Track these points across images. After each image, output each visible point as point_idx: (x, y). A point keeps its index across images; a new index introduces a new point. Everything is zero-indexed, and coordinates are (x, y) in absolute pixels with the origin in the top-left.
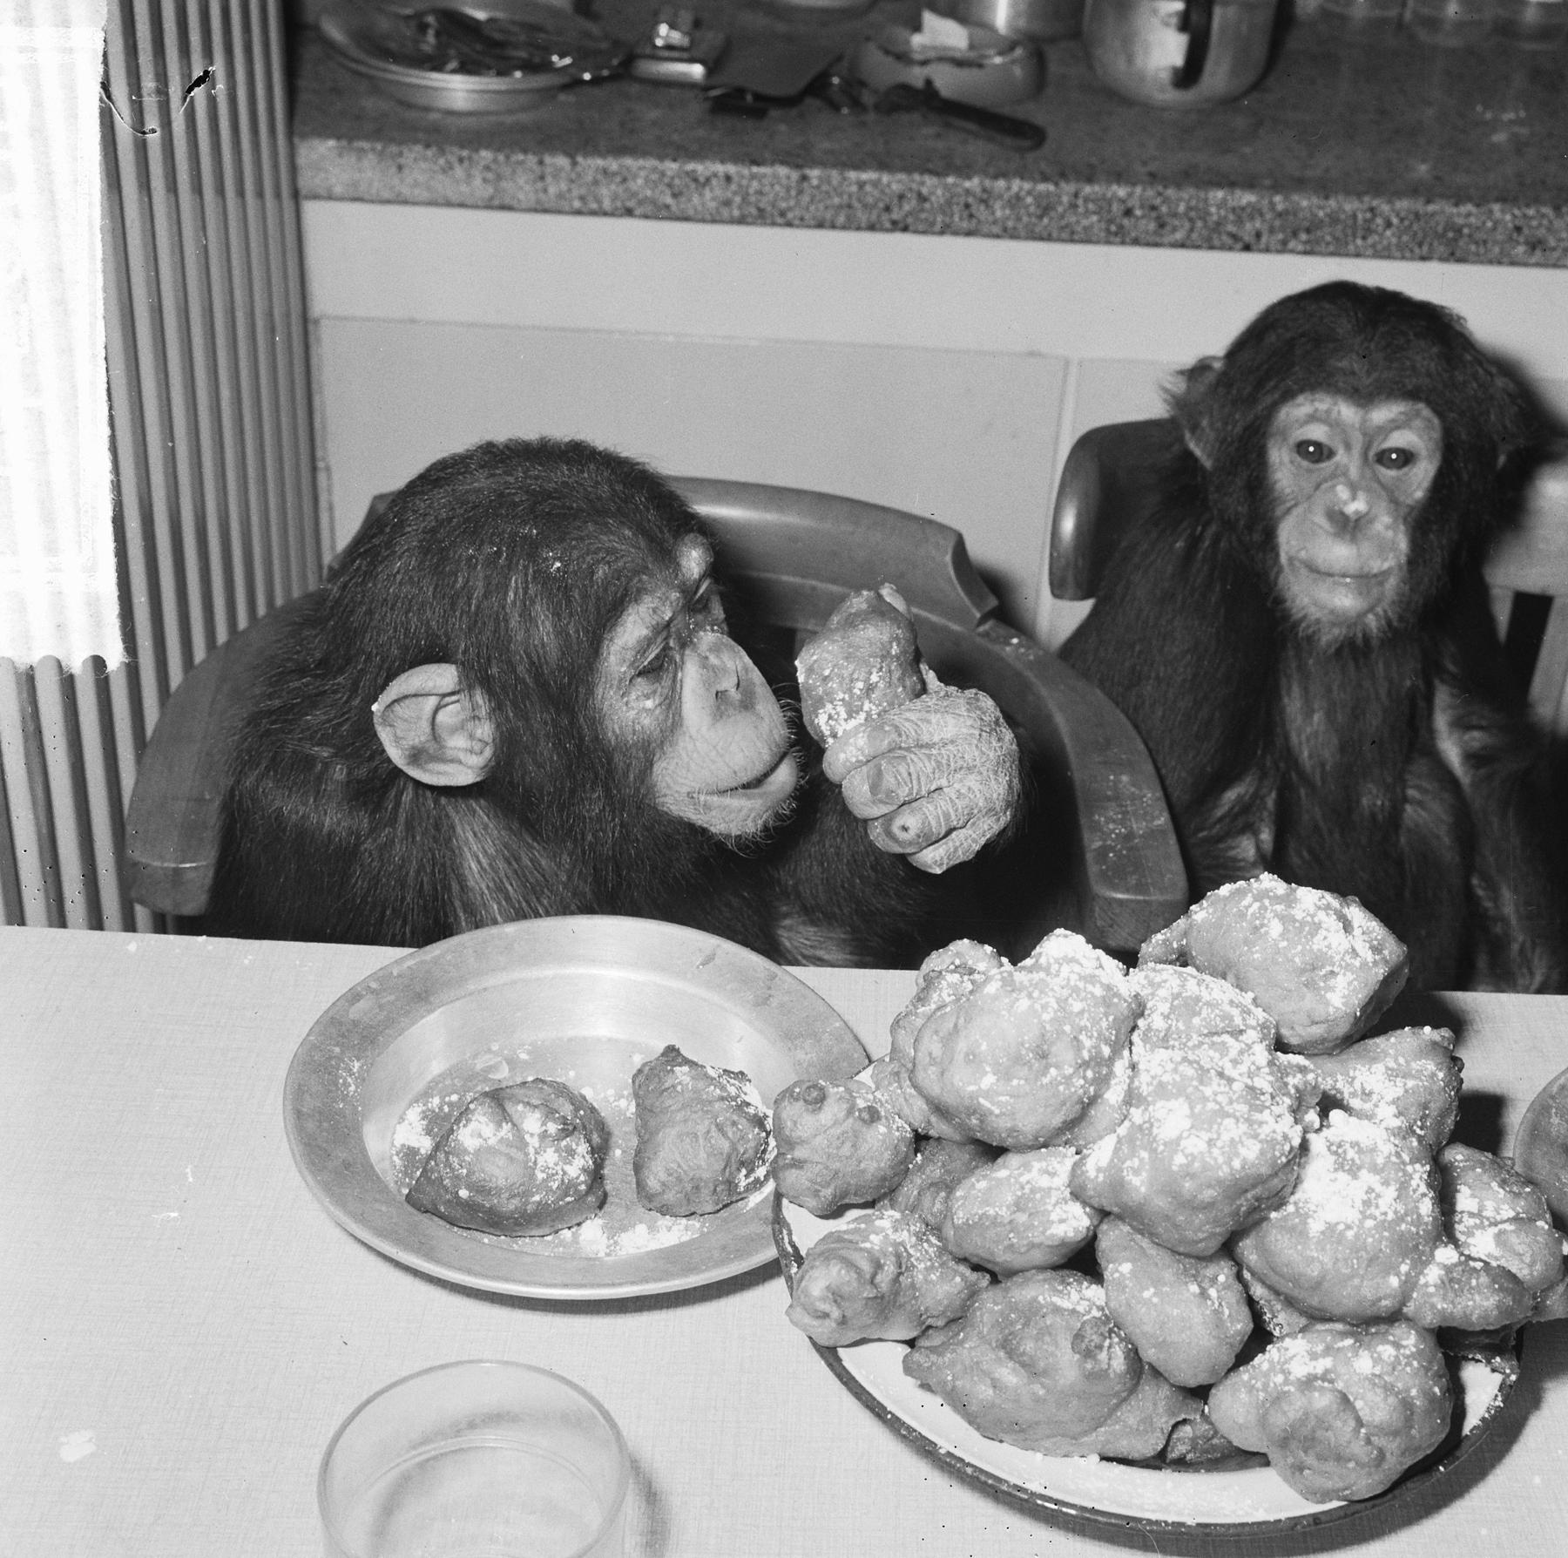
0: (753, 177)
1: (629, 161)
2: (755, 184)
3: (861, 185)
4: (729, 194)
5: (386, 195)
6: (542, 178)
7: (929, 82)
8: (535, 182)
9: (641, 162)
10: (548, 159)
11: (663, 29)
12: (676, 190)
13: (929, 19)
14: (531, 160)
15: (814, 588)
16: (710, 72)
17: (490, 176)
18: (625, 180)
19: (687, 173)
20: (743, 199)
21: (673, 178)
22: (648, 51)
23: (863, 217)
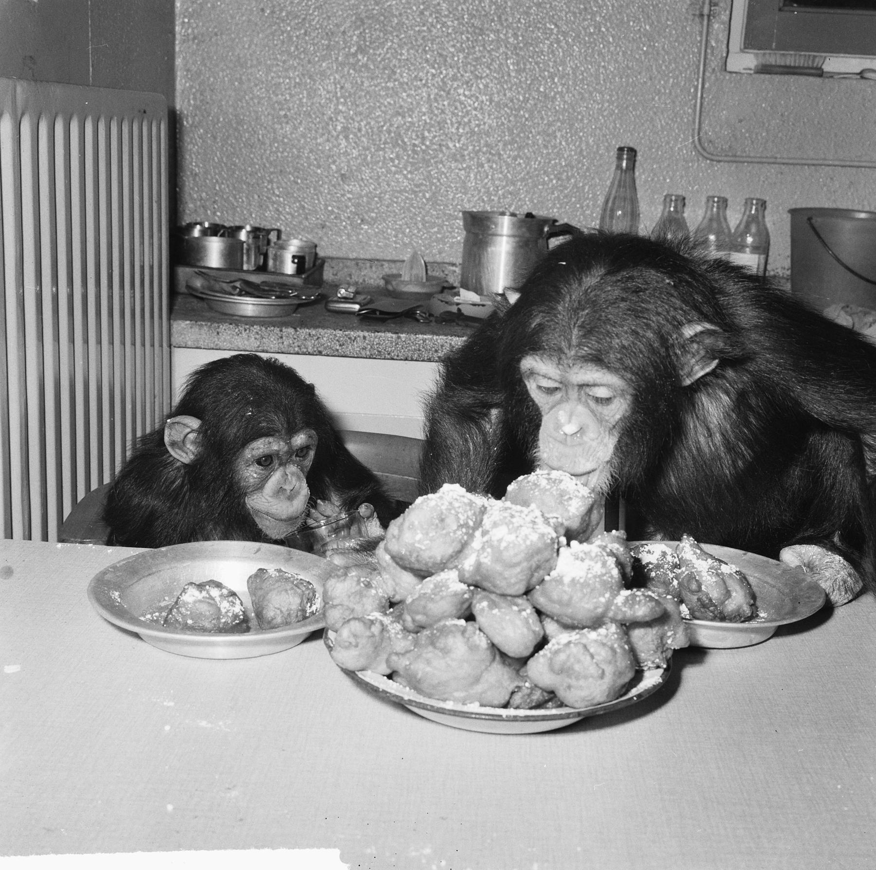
0: (376, 337)
1: (320, 330)
2: (377, 340)
3: (424, 341)
4: (365, 344)
5: (212, 346)
6: (281, 337)
7: (459, 310)
9: (326, 330)
10: (284, 330)
11: (343, 291)
13: (463, 291)
14: (277, 330)
15: (387, 477)
16: (361, 306)
17: (257, 336)
18: (318, 338)
20: (371, 347)
21: (340, 337)
22: (335, 299)
23: (425, 355)
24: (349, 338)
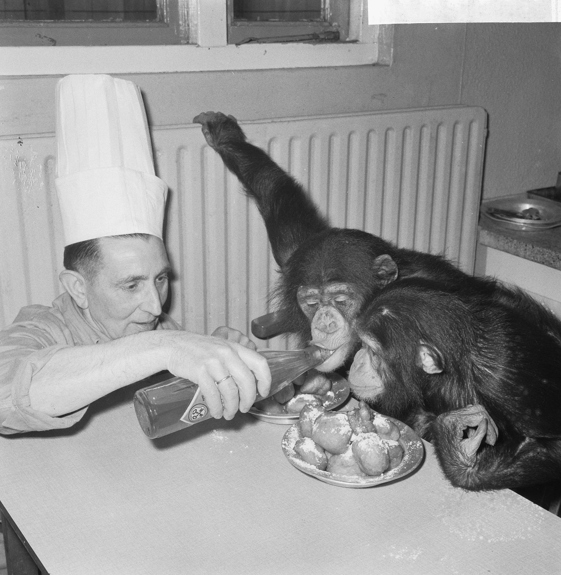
6: (526, 250)
8: (524, 250)
12: (554, 260)
17: (515, 247)
18: (543, 254)
19: (557, 256)
21: (554, 256)
24: (558, 258)
